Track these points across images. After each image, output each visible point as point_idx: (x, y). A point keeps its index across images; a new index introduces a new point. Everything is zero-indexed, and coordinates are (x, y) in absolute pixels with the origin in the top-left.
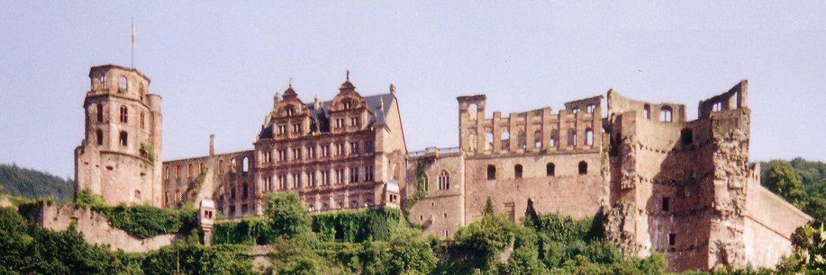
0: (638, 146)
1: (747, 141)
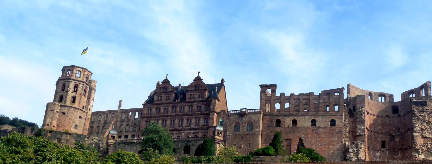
0: (366, 113)
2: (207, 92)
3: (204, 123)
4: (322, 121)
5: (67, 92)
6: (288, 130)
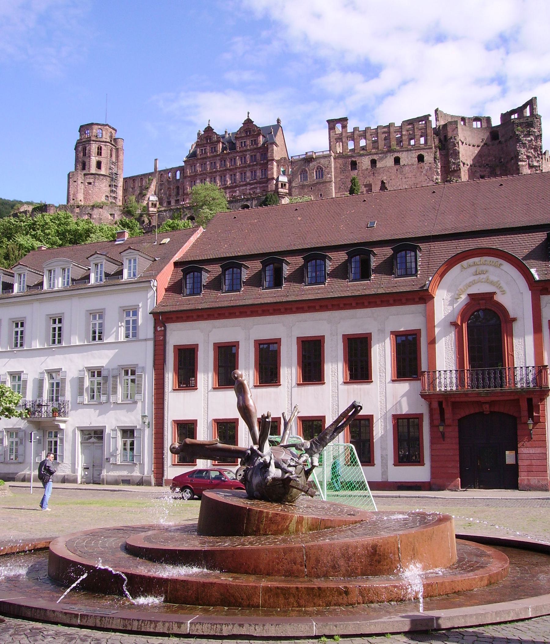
0: (460, 143)
1: (541, 135)
2: (261, 137)
3: (262, 175)
4: (408, 158)
5: (90, 157)
6: (366, 172)
